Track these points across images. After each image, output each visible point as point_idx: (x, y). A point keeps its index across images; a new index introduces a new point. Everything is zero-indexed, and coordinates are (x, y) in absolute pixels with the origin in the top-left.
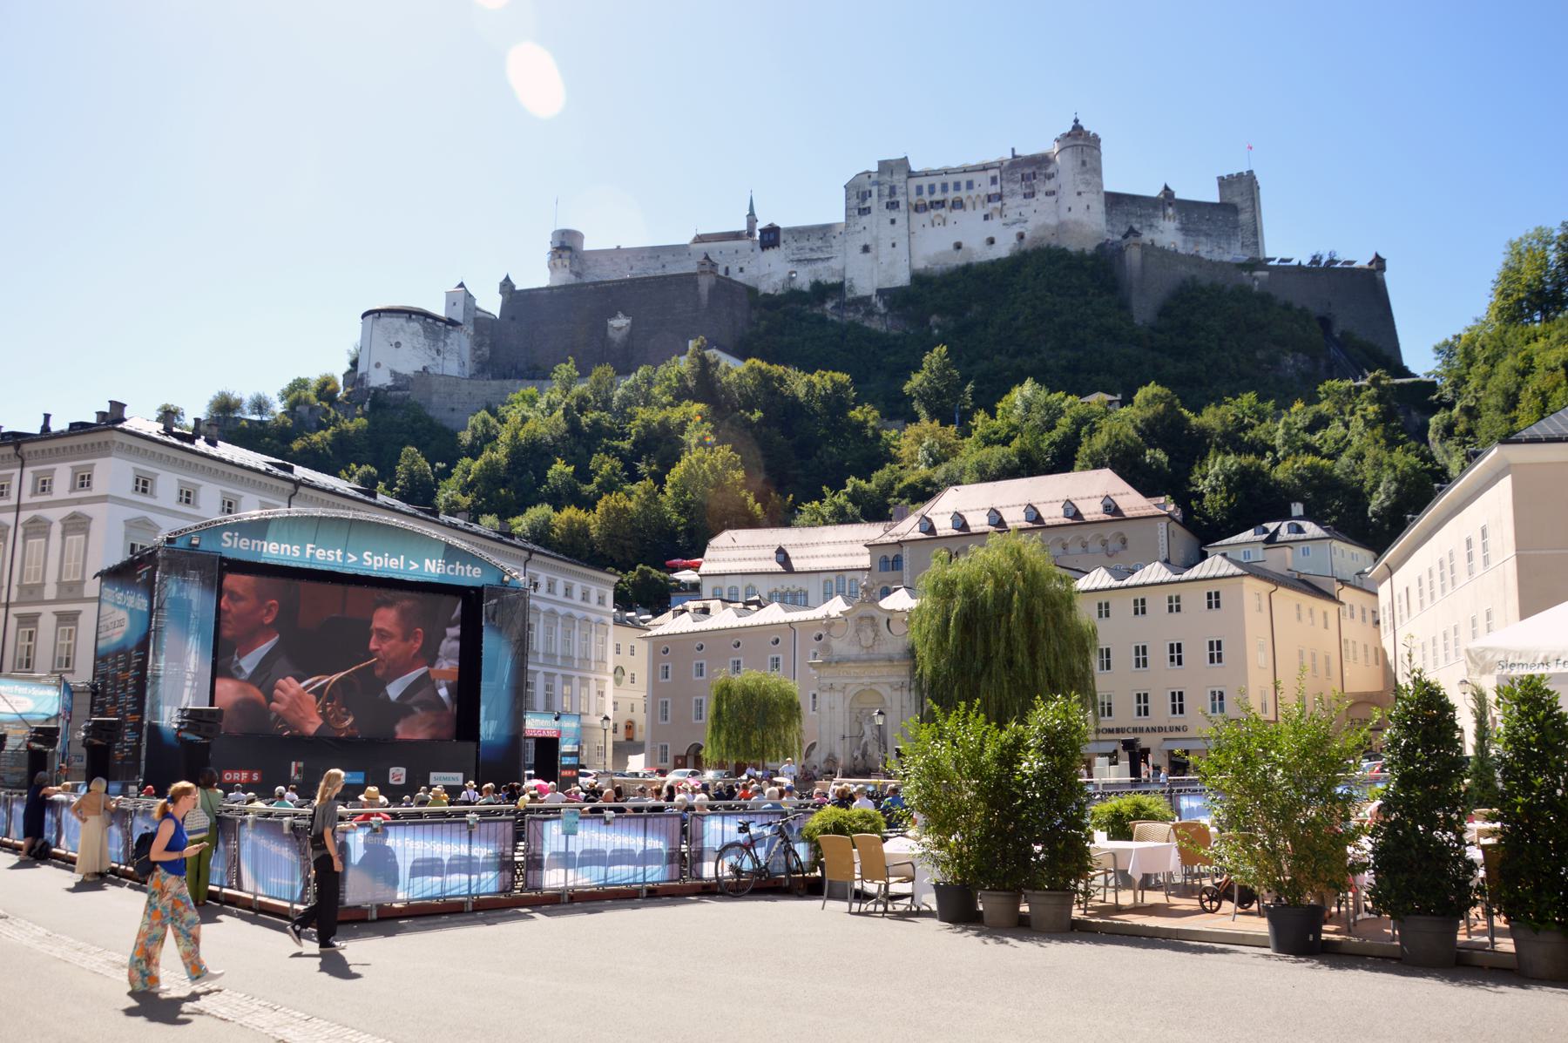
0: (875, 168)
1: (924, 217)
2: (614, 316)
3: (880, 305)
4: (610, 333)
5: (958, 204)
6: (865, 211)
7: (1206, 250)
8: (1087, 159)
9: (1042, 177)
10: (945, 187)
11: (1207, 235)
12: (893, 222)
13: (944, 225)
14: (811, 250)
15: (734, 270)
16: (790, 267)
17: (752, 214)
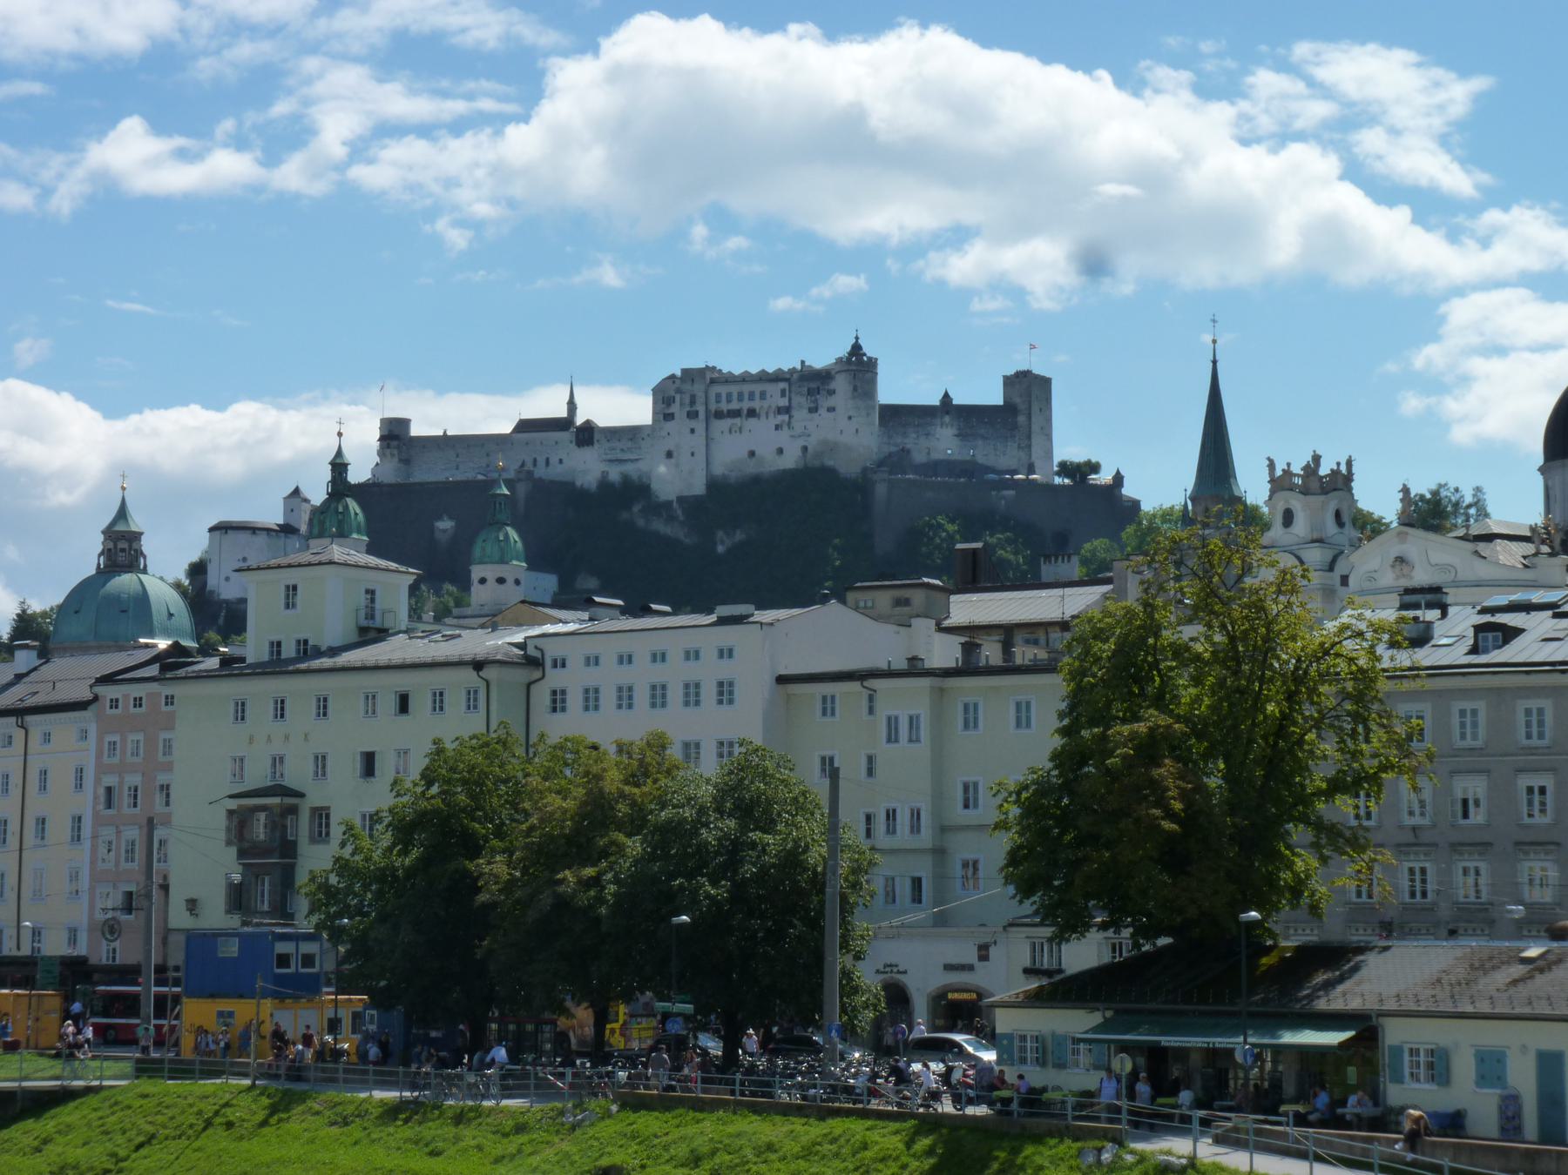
0: (679, 373)
1: (725, 424)
2: (440, 518)
3: (679, 512)
4: (438, 535)
5: (752, 413)
6: (669, 417)
7: (984, 453)
8: (859, 385)
9: (825, 393)
10: (740, 396)
11: (984, 438)
12: (692, 431)
13: (741, 432)
14: (622, 450)
15: (554, 460)
16: (603, 467)
17: (572, 405)
